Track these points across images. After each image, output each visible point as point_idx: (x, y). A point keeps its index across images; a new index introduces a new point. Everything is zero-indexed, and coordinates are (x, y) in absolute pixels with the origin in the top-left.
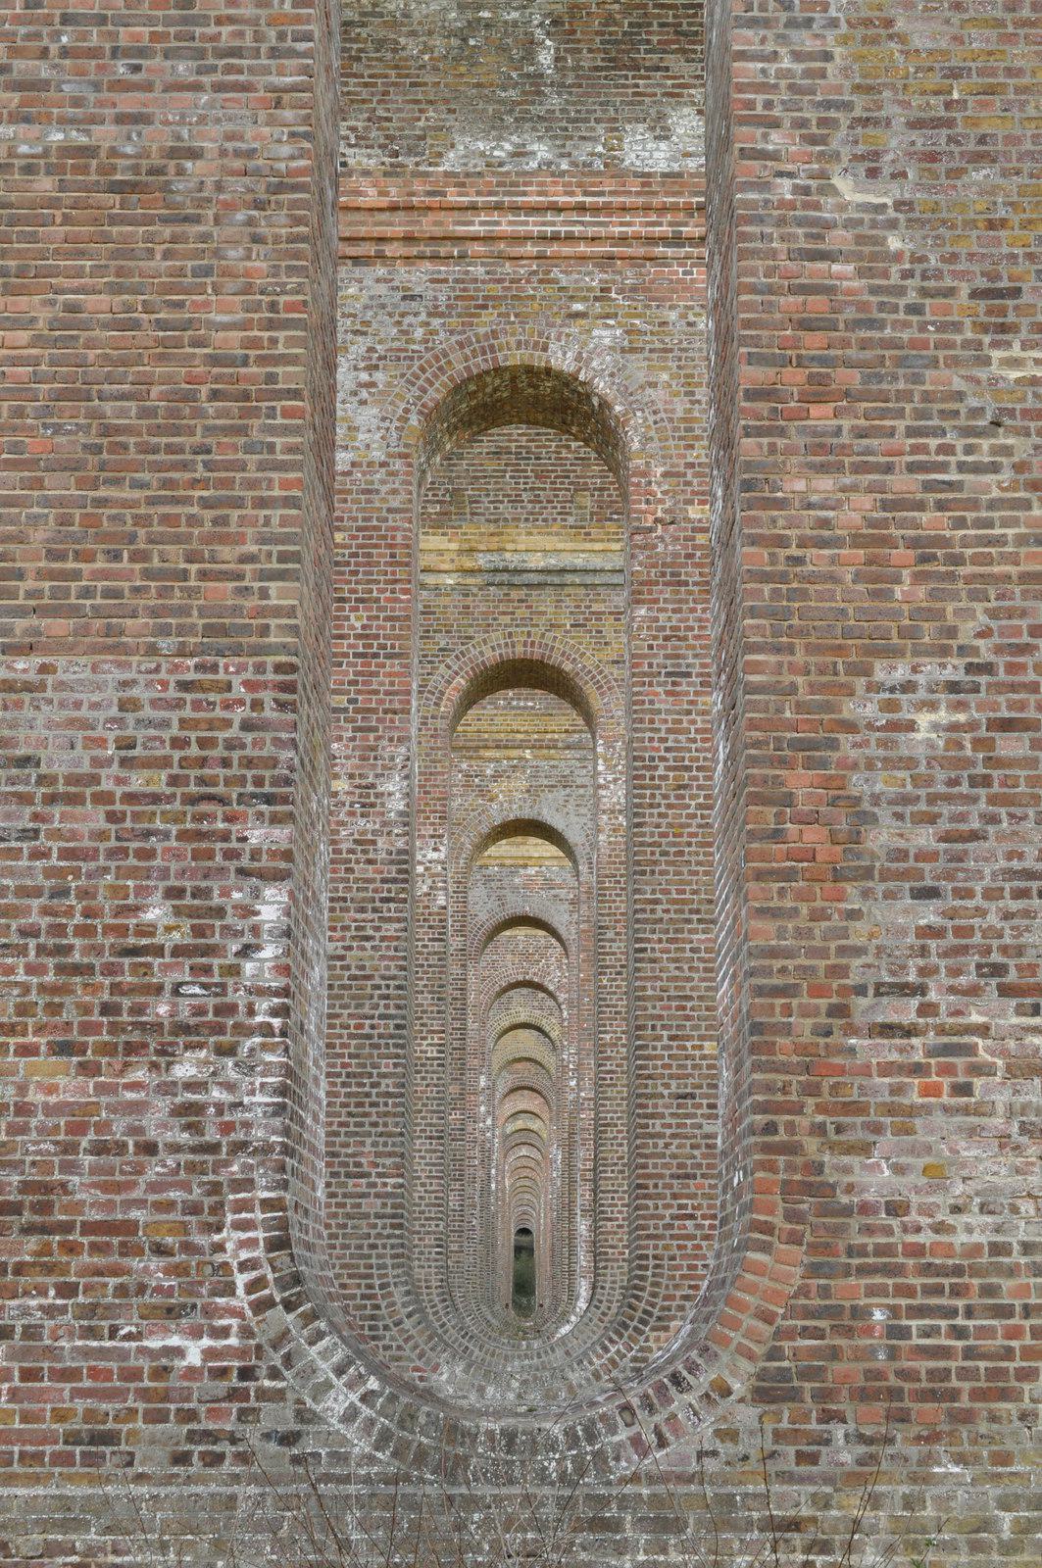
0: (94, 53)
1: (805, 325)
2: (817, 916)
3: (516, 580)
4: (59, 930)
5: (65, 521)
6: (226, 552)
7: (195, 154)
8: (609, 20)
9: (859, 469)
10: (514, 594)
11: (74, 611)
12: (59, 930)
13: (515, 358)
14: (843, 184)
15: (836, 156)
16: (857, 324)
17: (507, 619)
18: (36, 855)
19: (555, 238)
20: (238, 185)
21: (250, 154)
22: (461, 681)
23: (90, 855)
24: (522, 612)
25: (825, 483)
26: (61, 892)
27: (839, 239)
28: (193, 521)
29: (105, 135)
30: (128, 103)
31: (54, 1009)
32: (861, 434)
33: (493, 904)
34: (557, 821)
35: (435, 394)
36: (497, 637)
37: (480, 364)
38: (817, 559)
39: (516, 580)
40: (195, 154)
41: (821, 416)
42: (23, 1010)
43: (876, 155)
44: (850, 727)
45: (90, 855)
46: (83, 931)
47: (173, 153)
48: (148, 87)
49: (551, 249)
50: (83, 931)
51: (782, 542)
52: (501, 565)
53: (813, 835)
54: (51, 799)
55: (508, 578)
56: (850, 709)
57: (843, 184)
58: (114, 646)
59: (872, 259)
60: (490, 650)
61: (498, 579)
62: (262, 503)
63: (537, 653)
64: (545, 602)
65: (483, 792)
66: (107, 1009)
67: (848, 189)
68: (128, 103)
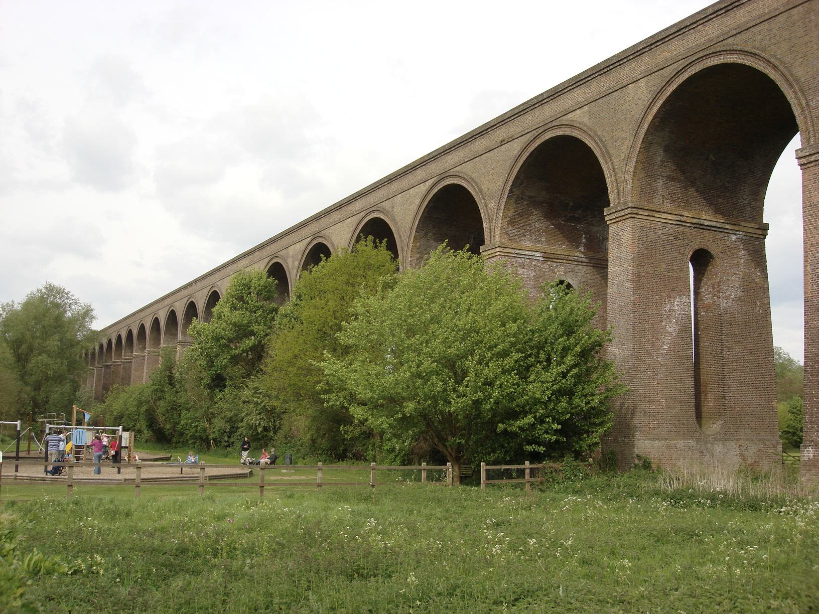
3: (702, 227)
10: (701, 231)
17: (699, 237)
24: (702, 236)
39: (702, 227)
52: (699, 223)
55: (699, 226)
61: (698, 226)
64: (706, 233)
65: (553, 272)
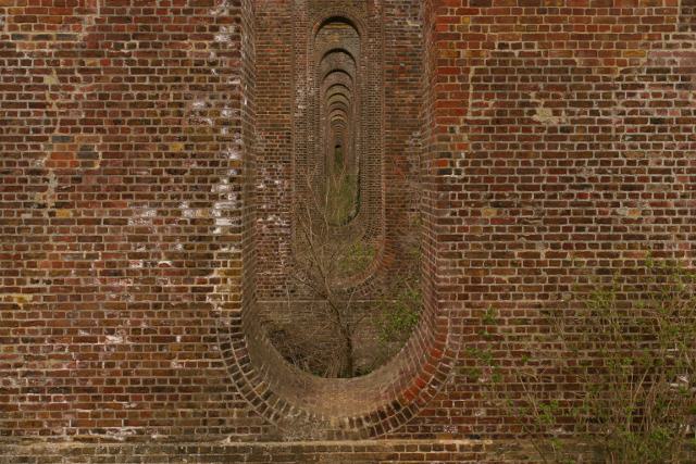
6: (275, 108)
7: (265, 15)
9: (410, 88)
14: (409, 22)
15: (406, 15)
16: (411, 55)
21: (276, 15)
25: (403, 92)
27: (408, 35)
32: (412, 80)
33: (328, 65)
34: (349, 50)
36: (329, 9)
38: (402, 109)
40: (265, 15)
41: (403, 77)
43: (416, 15)
44: (407, 146)
51: (393, 105)
56: (407, 142)
57: (409, 22)
59: (415, 40)
67: (410, 23)
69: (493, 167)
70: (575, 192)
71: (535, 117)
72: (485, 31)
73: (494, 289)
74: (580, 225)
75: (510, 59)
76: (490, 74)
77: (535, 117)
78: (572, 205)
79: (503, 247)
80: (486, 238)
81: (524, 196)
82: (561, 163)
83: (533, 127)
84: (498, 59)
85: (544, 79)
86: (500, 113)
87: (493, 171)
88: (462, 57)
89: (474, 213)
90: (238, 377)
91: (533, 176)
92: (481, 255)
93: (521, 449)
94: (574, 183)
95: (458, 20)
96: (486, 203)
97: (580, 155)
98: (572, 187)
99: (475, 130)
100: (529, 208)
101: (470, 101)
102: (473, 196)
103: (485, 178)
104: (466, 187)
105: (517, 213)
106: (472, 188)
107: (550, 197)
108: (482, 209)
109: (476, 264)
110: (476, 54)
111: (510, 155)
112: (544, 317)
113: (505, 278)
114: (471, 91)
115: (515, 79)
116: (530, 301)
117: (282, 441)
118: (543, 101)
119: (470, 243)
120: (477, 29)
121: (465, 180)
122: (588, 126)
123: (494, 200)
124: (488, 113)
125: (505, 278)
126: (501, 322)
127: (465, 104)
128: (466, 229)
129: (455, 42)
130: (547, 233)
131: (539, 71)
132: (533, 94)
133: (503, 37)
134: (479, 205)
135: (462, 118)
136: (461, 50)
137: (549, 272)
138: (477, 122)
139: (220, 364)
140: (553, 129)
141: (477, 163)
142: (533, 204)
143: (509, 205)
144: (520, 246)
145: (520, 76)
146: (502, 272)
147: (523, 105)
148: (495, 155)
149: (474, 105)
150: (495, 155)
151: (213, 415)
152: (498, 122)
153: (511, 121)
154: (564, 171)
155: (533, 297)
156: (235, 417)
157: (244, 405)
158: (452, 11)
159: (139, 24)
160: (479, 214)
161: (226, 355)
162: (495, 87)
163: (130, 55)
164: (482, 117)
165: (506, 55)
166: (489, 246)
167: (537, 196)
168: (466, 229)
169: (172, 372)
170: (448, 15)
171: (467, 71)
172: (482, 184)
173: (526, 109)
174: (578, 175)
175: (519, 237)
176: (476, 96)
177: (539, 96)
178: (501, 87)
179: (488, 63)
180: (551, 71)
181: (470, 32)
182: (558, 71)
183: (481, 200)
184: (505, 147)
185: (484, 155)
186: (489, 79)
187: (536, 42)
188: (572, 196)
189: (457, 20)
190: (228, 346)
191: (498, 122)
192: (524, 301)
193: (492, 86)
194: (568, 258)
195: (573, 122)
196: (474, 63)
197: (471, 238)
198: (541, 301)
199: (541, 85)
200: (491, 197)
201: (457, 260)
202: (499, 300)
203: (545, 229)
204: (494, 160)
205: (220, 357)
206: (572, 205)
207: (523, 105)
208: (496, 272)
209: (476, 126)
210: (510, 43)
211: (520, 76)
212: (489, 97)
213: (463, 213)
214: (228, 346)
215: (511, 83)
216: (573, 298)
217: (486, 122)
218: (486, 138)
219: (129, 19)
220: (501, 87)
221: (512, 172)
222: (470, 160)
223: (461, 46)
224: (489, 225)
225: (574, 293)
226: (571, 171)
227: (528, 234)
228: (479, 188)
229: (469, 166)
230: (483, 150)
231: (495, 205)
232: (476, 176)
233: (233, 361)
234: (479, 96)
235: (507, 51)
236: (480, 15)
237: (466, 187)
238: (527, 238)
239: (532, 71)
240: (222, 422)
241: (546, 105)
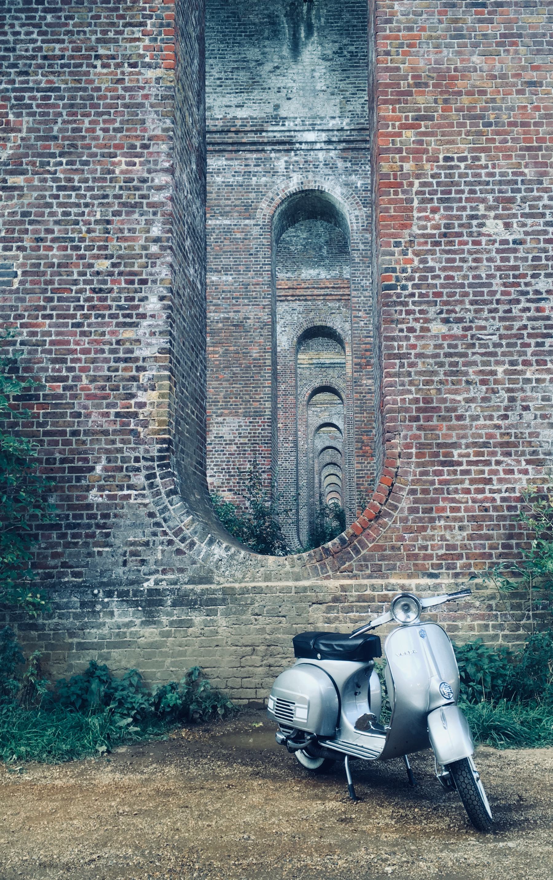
0: (229, 298)
1: (366, 351)
2: (368, 463)
4: (228, 469)
5: (227, 391)
6: (257, 397)
7: (249, 319)
8: (339, 241)
11: (229, 409)
12: (228, 469)
13: (319, 324)
18: (224, 454)
19: (327, 295)
20: (257, 324)
22: (310, 392)
23: (233, 454)
24: (325, 374)
26: (229, 462)
28: (251, 391)
29: (231, 315)
30: (236, 308)
31: (228, 483)
34: (337, 423)
35: (300, 333)
37: (310, 325)
38: (368, 396)
40: (249, 319)
42: (223, 483)
45: (233, 454)
46: (233, 469)
47: (245, 318)
48: (239, 305)
49: (327, 297)
50: (233, 469)
51: (362, 393)
53: (367, 448)
54: (226, 444)
55: (321, 366)
58: (237, 415)
60: (317, 384)
62: (264, 387)
63: (328, 384)
64: (330, 371)
66: (238, 483)
68: (236, 308)
69: (442, 281)
70: (532, 306)
71: (484, 230)
72: (429, 144)
73: (448, 410)
74: (540, 340)
75: (456, 172)
76: (435, 188)
77: (484, 230)
78: (529, 319)
79: (456, 364)
80: (437, 356)
81: (476, 311)
82: (515, 277)
83: (484, 239)
84: (442, 172)
85: (493, 191)
86: (447, 226)
87: (443, 286)
88: (405, 171)
89: (422, 329)
90: (165, 509)
91: (485, 290)
92: (434, 373)
93: (486, 587)
94: (531, 296)
95: (400, 135)
96: (435, 319)
97: (535, 267)
98: (529, 301)
99: (419, 244)
100: (483, 323)
101: (416, 214)
102: (421, 312)
103: (433, 293)
104: (414, 303)
105: (470, 328)
106: (420, 303)
107: (505, 312)
108: (431, 326)
109: (427, 383)
110: (422, 168)
111: (460, 269)
112: (506, 439)
113: (458, 398)
114: (416, 204)
115: (462, 192)
116: (488, 422)
117: (212, 583)
118: (492, 214)
119: (420, 361)
120: (421, 142)
121: (412, 295)
122: (541, 238)
123: (444, 316)
124: (436, 227)
125: (458, 398)
126: (455, 445)
127: (410, 218)
128: (414, 347)
129: (397, 156)
130: (503, 349)
131: (488, 183)
132: (482, 206)
133: (448, 150)
134: (427, 321)
135: (406, 232)
136: (404, 164)
137: (509, 390)
138: (423, 236)
139: (143, 496)
140: (504, 242)
141: (426, 278)
142: (486, 319)
143: (460, 320)
144: (475, 363)
145: (467, 189)
146: (456, 392)
147: (472, 217)
148: (444, 269)
149: (419, 218)
150: (444, 269)
151: (134, 554)
152: (445, 235)
153: (460, 235)
154: (519, 285)
155: (491, 418)
156: (159, 556)
157: (170, 542)
158: (393, 125)
159: (67, 143)
160: (428, 330)
161: (151, 486)
162: (440, 200)
163: (55, 172)
164: (429, 231)
165: (451, 167)
166: (441, 365)
167: (490, 311)
168: (414, 347)
169: (89, 506)
170: (390, 129)
171: (411, 184)
172: (431, 298)
173: (475, 222)
174: (534, 288)
175: (474, 354)
176: (420, 210)
177: (489, 208)
178: (448, 200)
179: (433, 176)
180: (500, 183)
181: (412, 146)
182: (509, 182)
183: (431, 315)
184: (454, 260)
185: (432, 269)
186: (435, 192)
187: (483, 155)
188: (528, 309)
189: (400, 135)
190: (154, 476)
191: (445, 235)
192: (482, 422)
193: (438, 199)
194: (528, 375)
195: (526, 233)
196: (418, 176)
197: (420, 356)
198: (500, 422)
199: (490, 197)
200: (441, 312)
201: (407, 379)
202: (454, 422)
203: (501, 345)
204: (443, 275)
205: (144, 489)
206: (529, 319)
207: (472, 217)
208: (450, 392)
209: (422, 240)
210: (455, 156)
211: (467, 189)
212: (434, 210)
213: (411, 330)
214: (154, 476)
215: (458, 196)
216: (535, 418)
217: (433, 236)
218: (433, 253)
219: (56, 138)
220: (448, 200)
221: (462, 286)
222: (417, 275)
223: (402, 159)
224: (440, 342)
225: (538, 413)
226: (526, 284)
227: (483, 350)
228: (428, 302)
229: (416, 281)
230: (431, 264)
231: (446, 321)
232: (424, 291)
233: (158, 493)
234: (425, 210)
235: (453, 163)
236: (423, 129)
237: (414, 303)
238: (482, 355)
239: (480, 183)
240: (143, 562)
241: (496, 217)
